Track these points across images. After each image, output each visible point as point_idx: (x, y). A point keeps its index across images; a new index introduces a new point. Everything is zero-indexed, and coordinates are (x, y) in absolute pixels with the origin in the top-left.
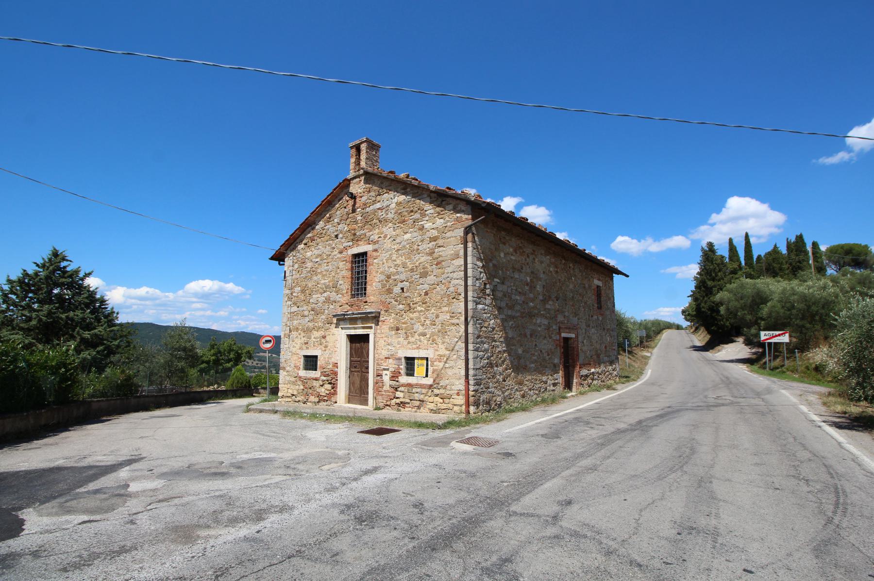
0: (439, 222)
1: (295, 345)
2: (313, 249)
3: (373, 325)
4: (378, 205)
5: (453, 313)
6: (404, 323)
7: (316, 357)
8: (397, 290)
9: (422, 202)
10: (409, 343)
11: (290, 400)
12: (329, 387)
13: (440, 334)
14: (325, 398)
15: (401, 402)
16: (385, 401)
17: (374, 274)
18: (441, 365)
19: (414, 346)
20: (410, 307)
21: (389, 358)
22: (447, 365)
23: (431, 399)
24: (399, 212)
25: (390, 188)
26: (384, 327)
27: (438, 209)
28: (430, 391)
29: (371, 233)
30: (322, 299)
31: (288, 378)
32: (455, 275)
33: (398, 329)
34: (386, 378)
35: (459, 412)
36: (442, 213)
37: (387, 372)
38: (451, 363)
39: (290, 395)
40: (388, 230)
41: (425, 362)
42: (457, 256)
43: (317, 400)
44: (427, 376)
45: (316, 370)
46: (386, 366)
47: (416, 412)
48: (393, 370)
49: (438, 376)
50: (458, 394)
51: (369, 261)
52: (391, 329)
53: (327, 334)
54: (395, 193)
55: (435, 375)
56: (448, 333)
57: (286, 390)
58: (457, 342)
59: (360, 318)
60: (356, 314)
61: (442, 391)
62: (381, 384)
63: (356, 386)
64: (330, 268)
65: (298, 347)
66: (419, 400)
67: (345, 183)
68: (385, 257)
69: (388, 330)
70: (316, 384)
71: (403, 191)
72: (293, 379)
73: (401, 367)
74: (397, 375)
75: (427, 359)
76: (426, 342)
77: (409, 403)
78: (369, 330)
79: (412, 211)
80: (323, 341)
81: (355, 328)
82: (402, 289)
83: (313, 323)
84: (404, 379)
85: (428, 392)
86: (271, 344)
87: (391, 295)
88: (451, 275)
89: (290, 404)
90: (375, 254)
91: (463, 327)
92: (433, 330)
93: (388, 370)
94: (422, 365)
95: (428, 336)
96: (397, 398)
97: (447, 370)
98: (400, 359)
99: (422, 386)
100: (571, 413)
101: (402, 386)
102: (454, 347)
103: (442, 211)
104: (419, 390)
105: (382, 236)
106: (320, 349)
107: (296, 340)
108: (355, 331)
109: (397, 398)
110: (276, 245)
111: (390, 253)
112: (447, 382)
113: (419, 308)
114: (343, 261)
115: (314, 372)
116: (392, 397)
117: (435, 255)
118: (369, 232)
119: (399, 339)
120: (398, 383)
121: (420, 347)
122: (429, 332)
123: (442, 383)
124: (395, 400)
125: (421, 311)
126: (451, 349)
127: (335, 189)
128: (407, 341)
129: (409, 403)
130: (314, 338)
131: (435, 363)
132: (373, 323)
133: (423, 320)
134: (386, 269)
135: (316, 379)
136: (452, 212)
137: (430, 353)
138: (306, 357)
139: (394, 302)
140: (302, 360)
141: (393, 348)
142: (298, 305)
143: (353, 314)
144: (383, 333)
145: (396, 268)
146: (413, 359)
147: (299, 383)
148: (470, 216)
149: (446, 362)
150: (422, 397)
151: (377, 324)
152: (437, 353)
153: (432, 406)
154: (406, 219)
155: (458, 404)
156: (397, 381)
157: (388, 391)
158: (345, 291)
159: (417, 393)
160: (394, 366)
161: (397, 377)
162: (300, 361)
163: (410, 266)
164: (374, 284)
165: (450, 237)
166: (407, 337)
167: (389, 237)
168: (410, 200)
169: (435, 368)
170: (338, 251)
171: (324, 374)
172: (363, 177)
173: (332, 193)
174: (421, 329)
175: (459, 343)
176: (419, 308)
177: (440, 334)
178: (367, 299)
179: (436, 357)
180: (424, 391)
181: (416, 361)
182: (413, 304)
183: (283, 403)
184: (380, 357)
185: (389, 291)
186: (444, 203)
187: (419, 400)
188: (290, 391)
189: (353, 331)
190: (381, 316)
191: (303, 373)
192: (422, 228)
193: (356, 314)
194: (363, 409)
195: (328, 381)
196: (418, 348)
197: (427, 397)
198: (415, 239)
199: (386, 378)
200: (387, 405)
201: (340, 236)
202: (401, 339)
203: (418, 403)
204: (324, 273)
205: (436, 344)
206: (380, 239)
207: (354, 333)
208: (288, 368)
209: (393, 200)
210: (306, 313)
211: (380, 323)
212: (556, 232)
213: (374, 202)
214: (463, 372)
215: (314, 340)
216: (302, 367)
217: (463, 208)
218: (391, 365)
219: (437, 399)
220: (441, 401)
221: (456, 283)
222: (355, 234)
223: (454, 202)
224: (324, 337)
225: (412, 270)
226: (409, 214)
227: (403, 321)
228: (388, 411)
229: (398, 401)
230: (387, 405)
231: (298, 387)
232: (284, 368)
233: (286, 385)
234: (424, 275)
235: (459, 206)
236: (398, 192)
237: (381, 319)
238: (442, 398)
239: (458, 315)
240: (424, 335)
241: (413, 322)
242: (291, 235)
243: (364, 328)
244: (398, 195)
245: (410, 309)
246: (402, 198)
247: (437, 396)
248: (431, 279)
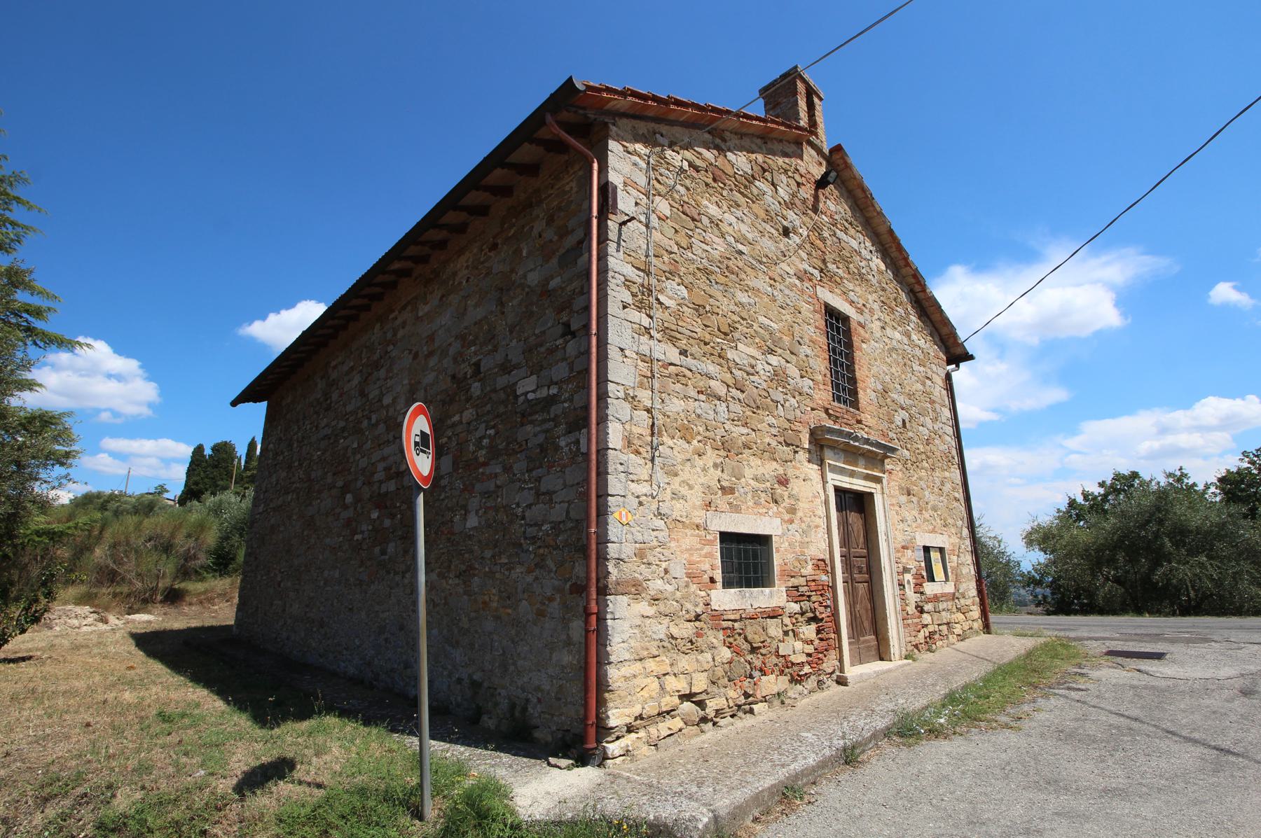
1: (684, 491)
7: (763, 541)
12: (809, 631)
31: (660, 629)
53: (790, 472)
57: (655, 685)
70: (774, 628)
72: (684, 630)
78: (873, 485)
81: (852, 474)
106: (778, 514)
107: (686, 473)
115: (767, 590)
130: (756, 479)
135: (774, 615)
138: (725, 537)
140: (716, 549)
143: (867, 441)
147: (715, 638)
162: (709, 555)
171: (795, 594)
189: (847, 479)
191: (727, 599)
193: (872, 444)
195: (802, 614)
207: (848, 486)
208: (657, 585)
212: (77, 337)
224: (783, 482)
231: (708, 656)
232: (636, 589)
233: (651, 664)
243: (868, 478)
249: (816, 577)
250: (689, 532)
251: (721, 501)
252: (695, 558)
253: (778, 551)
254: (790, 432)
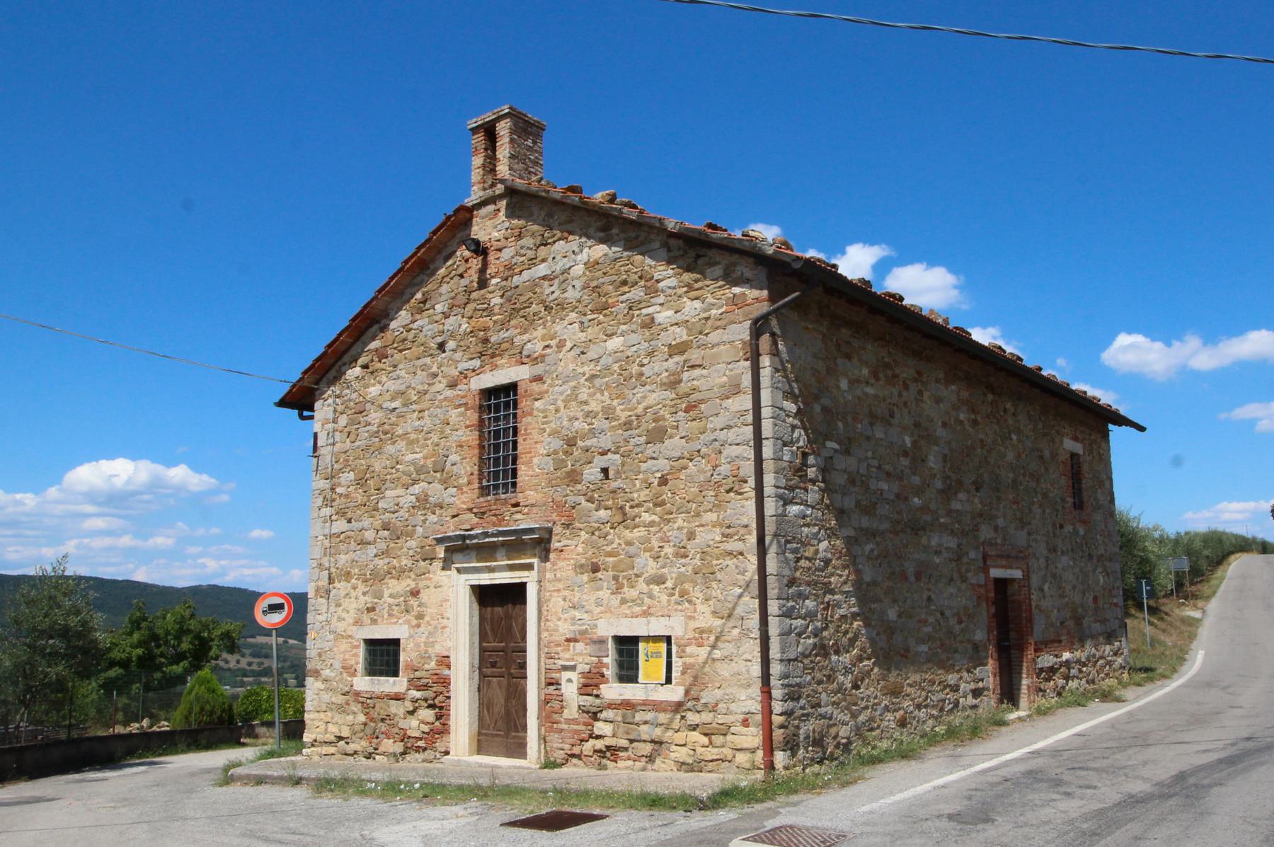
0: (691, 308)
1: (344, 615)
2: (384, 379)
3: (535, 561)
4: (542, 270)
5: (729, 527)
6: (610, 554)
7: (396, 642)
8: (591, 473)
9: (649, 261)
10: (624, 601)
11: (332, 750)
12: (429, 715)
13: (699, 578)
14: (421, 743)
15: (608, 748)
16: (567, 747)
17: (535, 435)
18: (703, 652)
19: (637, 609)
20: (625, 514)
21: (576, 640)
22: (717, 654)
23: (680, 737)
24: (594, 284)
25: (569, 227)
26: (561, 564)
27: (687, 277)
28: (678, 716)
29: (525, 337)
30: (408, 499)
31: (326, 697)
32: (731, 435)
33: (595, 569)
34: (570, 688)
35: (748, 765)
36: (697, 286)
37: (573, 675)
38: (725, 649)
39: (333, 738)
40: (568, 329)
41: (663, 647)
42: (735, 390)
43: (399, 748)
44: (669, 680)
45: (396, 674)
46: (568, 660)
47: (644, 769)
48: (587, 668)
49: (696, 682)
50: (745, 723)
51: (524, 404)
52: (580, 568)
53: (421, 584)
54: (584, 239)
55: (689, 679)
56: (719, 576)
57: (323, 727)
58: (740, 596)
59: (504, 544)
60: (493, 535)
61: (706, 717)
62: (556, 705)
63: (496, 710)
64: (427, 422)
65: (350, 618)
66: (652, 741)
67: (461, 215)
68: (561, 394)
69: (571, 573)
70: (397, 709)
71: (602, 234)
72: (340, 699)
73: (605, 660)
74: (595, 681)
75: (668, 639)
76: (664, 598)
77: (626, 749)
78: (525, 573)
79: (624, 283)
80: (413, 602)
81: (491, 570)
82: (605, 471)
83: (387, 560)
84: (613, 691)
85: (671, 720)
86: (284, 614)
87: (579, 487)
88: (722, 435)
89: (333, 760)
90: (536, 387)
91: (754, 559)
92: (683, 569)
93: (573, 668)
94: (658, 655)
95: (669, 584)
96: (598, 737)
97: (718, 664)
98: (602, 641)
99: (657, 706)
100: (1017, 760)
101: (610, 706)
102: (734, 608)
103: (696, 281)
104: (649, 716)
105: (553, 343)
106: (408, 622)
107: (346, 603)
108: (492, 575)
109: (598, 737)
110: (293, 371)
111: (573, 384)
112: (718, 693)
113: (646, 517)
114: (460, 406)
115: (392, 679)
116: (585, 736)
117: (683, 388)
118: (520, 334)
119: (600, 593)
120: (598, 701)
121: (652, 610)
122: (671, 573)
123: (707, 697)
124: (592, 742)
125: (652, 524)
126: (726, 613)
127: (435, 232)
128: (619, 596)
129: (626, 749)
130: (391, 596)
131: (688, 649)
132: (534, 556)
133: (655, 544)
134: (565, 423)
135: (398, 698)
136: (721, 283)
137: (674, 626)
138: (371, 643)
139: (584, 503)
140: (361, 651)
141: (585, 616)
142: (349, 516)
143: (486, 534)
144: (560, 580)
145: (589, 420)
146: (634, 640)
147: (355, 707)
148: (765, 293)
149: (714, 647)
150: (657, 733)
151: (545, 559)
152: (693, 624)
153: (682, 754)
154: (610, 301)
155: (745, 745)
156: (597, 696)
157: (574, 721)
158: (465, 480)
159: (646, 723)
160: (588, 659)
161: (597, 686)
163: (623, 416)
164: (536, 461)
165: (718, 344)
166: (619, 588)
167: (569, 345)
168: (619, 255)
169: (688, 660)
170: (445, 381)
171: (415, 684)
172: (504, 202)
173: (428, 241)
174: (652, 568)
175: (746, 599)
176: (646, 517)
177: (699, 578)
178: (520, 498)
179: (691, 634)
180: (663, 717)
181: (642, 646)
182: (632, 507)
183: (316, 758)
184: (553, 638)
185: (574, 477)
186: (700, 261)
187: (652, 741)
188: (332, 728)
189: (486, 576)
190: (554, 538)
191: (363, 683)
192: (649, 323)
193: (493, 535)
194: (515, 767)
195: (426, 700)
196: (646, 614)
197: (670, 733)
198: (634, 349)
199: (570, 688)
200: (573, 756)
201: (451, 345)
202: (605, 594)
203: (648, 748)
204: (413, 436)
205: (690, 602)
206: (548, 351)
207: (488, 582)
208: (326, 673)
209: (579, 257)
210: (369, 535)
211: (552, 556)
213: (533, 262)
214: (756, 670)
215: (391, 600)
216: (360, 667)
217: (748, 273)
218: (581, 656)
219: (696, 736)
220: (705, 740)
221: (734, 454)
222: (486, 341)
223: (726, 259)
224: (415, 593)
225: (627, 425)
226: (617, 289)
227: (609, 549)
228: (575, 769)
229: (599, 744)
230: (573, 756)
231: (351, 717)
232: (316, 673)
233: (322, 715)
234: (658, 435)
235: (738, 268)
236: (589, 237)
237: (555, 544)
238: (706, 735)
239: (742, 531)
240: (660, 580)
241: (632, 550)
242: (330, 346)
243: (512, 568)
244: (589, 243)
245: (624, 518)
246: (600, 250)
247: (694, 730)
248: (674, 445)
249: (438, 672)
250: (344, 641)
251: (366, 618)
252: (347, 657)
253: (404, 650)
254: (427, 548)
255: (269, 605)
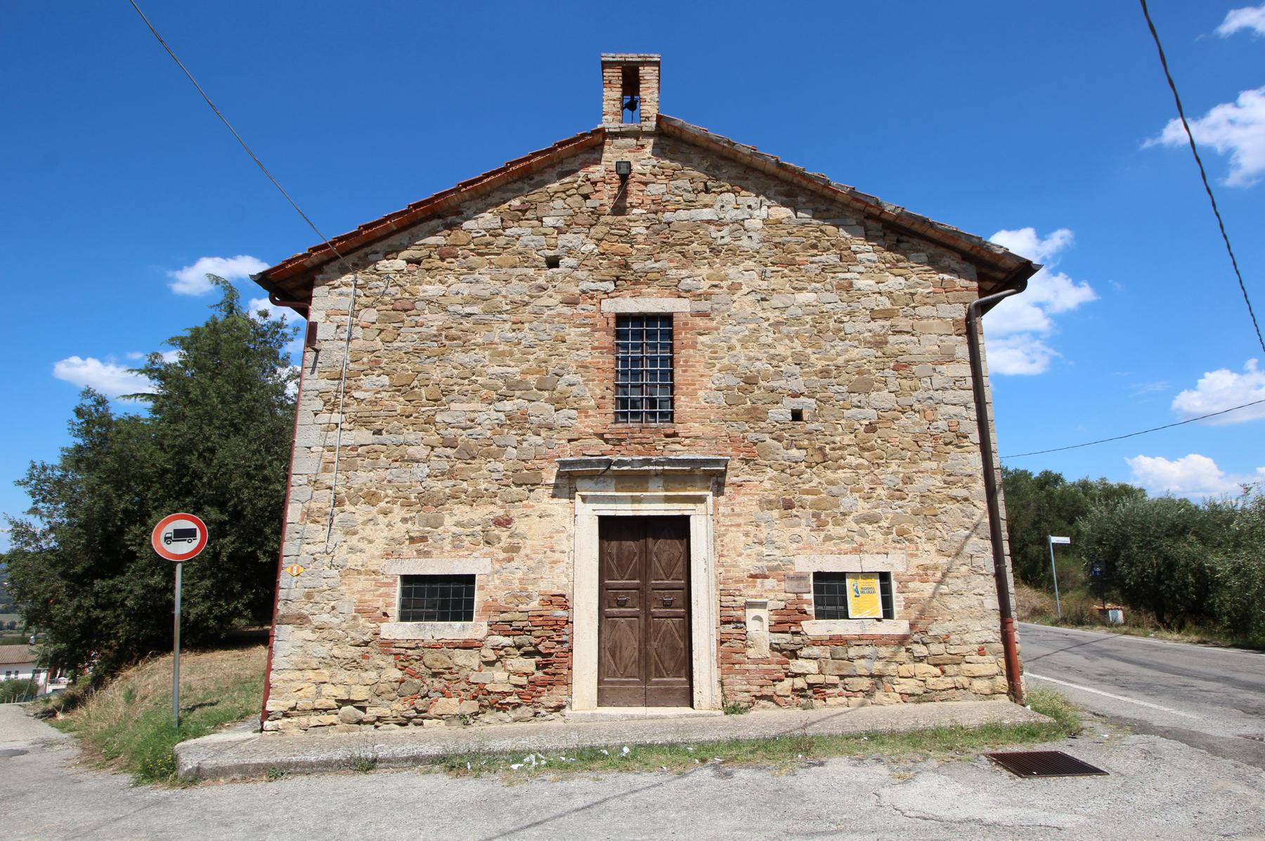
0: (893, 282)
2: (452, 279)
3: (709, 494)
4: (707, 214)
5: (949, 475)
6: (808, 492)
8: (781, 413)
9: (842, 232)
10: (828, 538)
11: (333, 718)
13: (920, 519)
14: (513, 699)
15: (811, 686)
16: (755, 688)
17: (701, 368)
18: (928, 588)
19: (846, 547)
20: (825, 455)
21: (766, 577)
22: (944, 589)
23: (903, 670)
24: (777, 240)
25: (744, 183)
26: (739, 499)
27: (888, 255)
28: (903, 649)
29: (684, 273)
30: (488, 415)
32: (949, 396)
33: (789, 506)
34: (759, 628)
35: (988, 691)
36: (901, 264)
37: (763, 613)
38: (954, 584)
39: (333, 703)
40: (745, 274)
41: (876, 583)
42: (951, 359)
43: (471, 707)
44: (888, 614)
45: (469, 617)
46: (752, 597)
47: (862, 705)
48: (782, 605)
49: (923, 616)
50: (981, 652)
51: (681, 337)
52: (768, 504)
53: (514, 513)
54: (762, 198)
55: (914, 614)
56: (943, 518)
58: (968, 537)
59: (663, 474)
60: (657, 463)
61: (936, 648)
62: (738, 645)
63: (626, 654)
64: (527, 336)
65: (380, 546)
66: (872, 676)
67: (598, 138)
68: (736, 333)
69: (757, 509)
71: (784, 199)
73: (806, 596)
74: (793, 618)
75: (884, 577)
76: (879, 537)
77: (835, 686)
79: (814, 246)
80: (503, 534)
81: (635, 500)
82: (797, 416)
83: (452, 482)
84: (816, 628)
85: (895, 653)
86: (195, 543)
87: (763, 424)
88: (938, 395)
89: (333, 733)
90: (701, 322)
91: (984, 506)
92: (899, 510)
93: (763, 605)
94: (870, 591)
95: (884, 524)
96: (796, 675)
97: (946, 599)
98: (801, 578)
99: (876, 641)
101: (816, 642)
102: (962, 548)
103: (898, 261)
104: (867, 651)
105: (724, 284)
106: (490, 555)
107: (368, 531)
108: (636, 506)
109: (796, 675)
110: (297, 246)
111: (753, 326)
112: (950, 626)
113: (853, 460)
114: (584, 325)
116: (781, 675)
117: (888, 349)
118: (677, 268)
119: (797, 530)
120: (797, 639)
121: (865, 548)
122: (887, 515)
123: (936, 629)
124: (788, 682)
125: (858, 467)
126: (953, 552)
127: (561, 145)
128: (822, 534)
129: (835, 686)
130: (458, 524)
131: (911, 585)
132: (707, 488)
133: (867, 487)
134: (743, 361)
135: (467, 646)
136: (927, 268)
137: (895, 563)
139: (769, 441)
141: (776, 552)
142: (378, 425)
144: (739, 515)
145: (775, 363)
146: (841, 576)
148: (975, 284)
149: (940, 582)
150: (877, 667)
151: (719, 492)
152: (915, 562)
153: (910, 686)
154: (797, 258)
155: (984, 673)
156: (797, 633)
157: (765, 660)
158: (593, 403)
159: (863, 657)
160: (782, 596)
161: (796, 623)
163: (820, 365)
164: (701, 393)
165: (928, 317)
166: (821, 526)
167: (745, 289)
168: (808, 221)
169: (911, 595)
170: (559, 297)
172: (652, 141)
173: (549, 150)
174: (863, 507)
175: (974, 539)
176: (853, 460)
177: (920, 519)
178: (679, 428)
179: (913, 571)
180: (884, 651)
181: (849, 582)
182: (834, 449)
183: (296, 733)
184: (730, 574)
185: (755, 415)
186: (903, 245)
187: (872, 676)
188: (327, 689)
189: (628, 506)
190: (729, 473)
191: (398, 630)
192: (848, 287)
194: (681, 717)
195: (519, 647)
196: (859, 550)
197: (893, 666)
198: (829, 306)
199: (759, 628)
200: (762, 697)
201: (567, 261)
202: (803, 531)
203: (866, 683)
204: (502, 348)
205: (911, 541)
206: (716, 290)
207: (630, 514)
209: (756, 213)
210: (419, 451)
211: (726, 490)
213: (690, 205)
214: (992, 602)
215: (458, 530)
216: (395, 611)
217: (954, 265)
218: (775, 594)
219: (923, 667)
220: (937, 671)
221: (952, 413)
222: (626, 266)
223: (932, 250)
224: (505, 522)
225: (825, 373)
226: (805, 249)
227: (806, 487)
228: (761, 711)
229: (800, 683)
230: (762, 697)
231: (373, 674)
232: (301, 620)
234: (865, 387)
235: (944, 259)
236: (769, 198)
237: (730, 478)
238: (935, 665)
239: (966, 480)
240: (873, 520)
241: (834, 489)
242: (366, 227)
243: (669, 500)
244: (768, 203)
245: (823, 460)
246: (783, 213)
247: (921, 661)
248: (883, 398)
249: (543, 613)
250: (362, 577)
251: (407, 549)
252: (368, 597)
253: (482, 588)
254: (526, 471)
255: (175, 531)
